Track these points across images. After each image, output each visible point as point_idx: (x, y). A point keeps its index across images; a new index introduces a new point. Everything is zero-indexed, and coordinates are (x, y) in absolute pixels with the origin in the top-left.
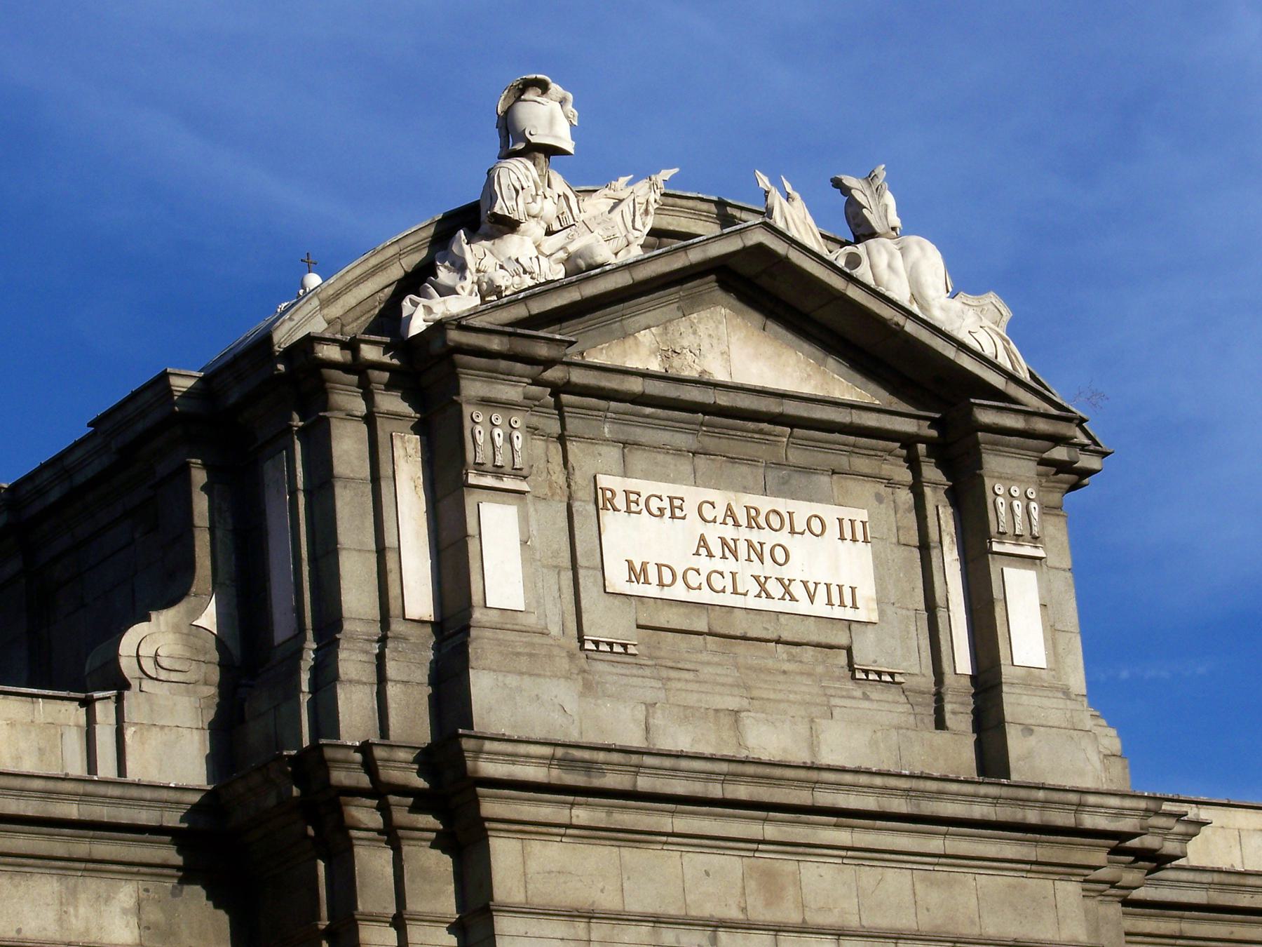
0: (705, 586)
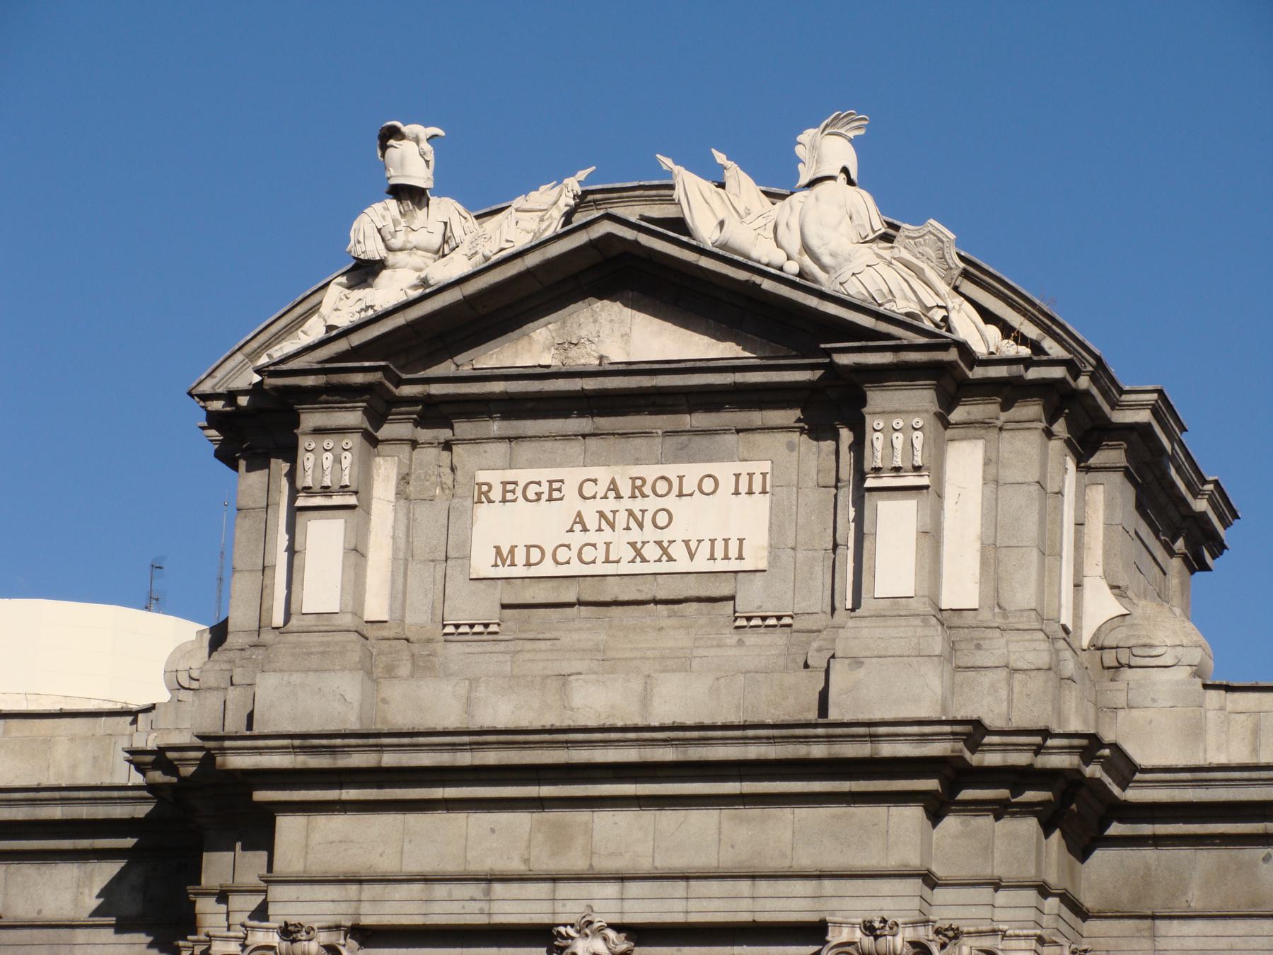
0: (575, 560)
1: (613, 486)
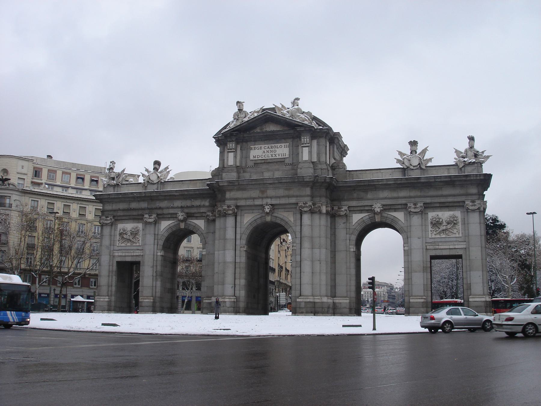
0: (264, 157)
1: (268, 147)
